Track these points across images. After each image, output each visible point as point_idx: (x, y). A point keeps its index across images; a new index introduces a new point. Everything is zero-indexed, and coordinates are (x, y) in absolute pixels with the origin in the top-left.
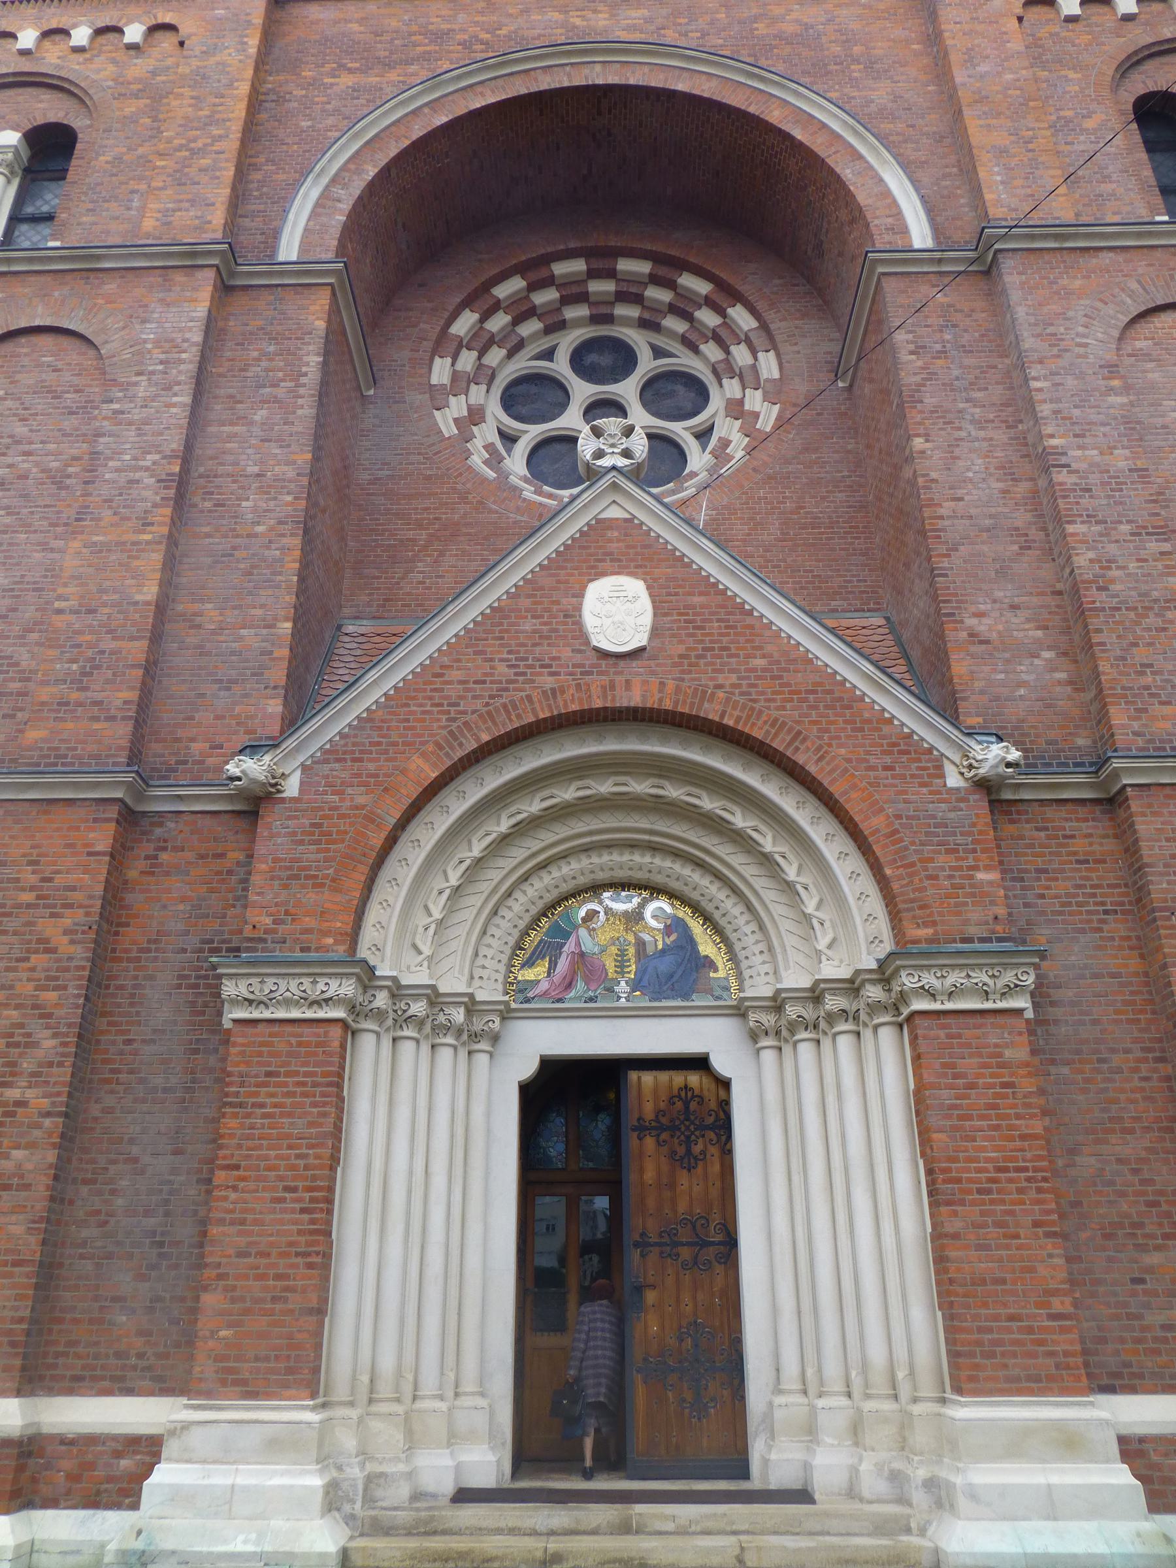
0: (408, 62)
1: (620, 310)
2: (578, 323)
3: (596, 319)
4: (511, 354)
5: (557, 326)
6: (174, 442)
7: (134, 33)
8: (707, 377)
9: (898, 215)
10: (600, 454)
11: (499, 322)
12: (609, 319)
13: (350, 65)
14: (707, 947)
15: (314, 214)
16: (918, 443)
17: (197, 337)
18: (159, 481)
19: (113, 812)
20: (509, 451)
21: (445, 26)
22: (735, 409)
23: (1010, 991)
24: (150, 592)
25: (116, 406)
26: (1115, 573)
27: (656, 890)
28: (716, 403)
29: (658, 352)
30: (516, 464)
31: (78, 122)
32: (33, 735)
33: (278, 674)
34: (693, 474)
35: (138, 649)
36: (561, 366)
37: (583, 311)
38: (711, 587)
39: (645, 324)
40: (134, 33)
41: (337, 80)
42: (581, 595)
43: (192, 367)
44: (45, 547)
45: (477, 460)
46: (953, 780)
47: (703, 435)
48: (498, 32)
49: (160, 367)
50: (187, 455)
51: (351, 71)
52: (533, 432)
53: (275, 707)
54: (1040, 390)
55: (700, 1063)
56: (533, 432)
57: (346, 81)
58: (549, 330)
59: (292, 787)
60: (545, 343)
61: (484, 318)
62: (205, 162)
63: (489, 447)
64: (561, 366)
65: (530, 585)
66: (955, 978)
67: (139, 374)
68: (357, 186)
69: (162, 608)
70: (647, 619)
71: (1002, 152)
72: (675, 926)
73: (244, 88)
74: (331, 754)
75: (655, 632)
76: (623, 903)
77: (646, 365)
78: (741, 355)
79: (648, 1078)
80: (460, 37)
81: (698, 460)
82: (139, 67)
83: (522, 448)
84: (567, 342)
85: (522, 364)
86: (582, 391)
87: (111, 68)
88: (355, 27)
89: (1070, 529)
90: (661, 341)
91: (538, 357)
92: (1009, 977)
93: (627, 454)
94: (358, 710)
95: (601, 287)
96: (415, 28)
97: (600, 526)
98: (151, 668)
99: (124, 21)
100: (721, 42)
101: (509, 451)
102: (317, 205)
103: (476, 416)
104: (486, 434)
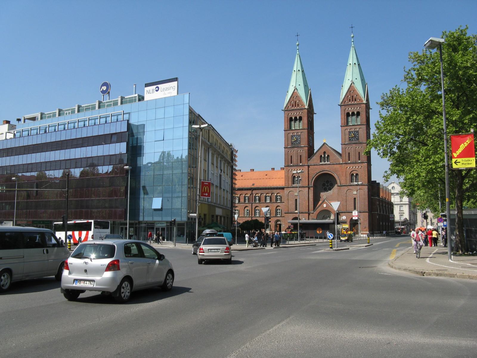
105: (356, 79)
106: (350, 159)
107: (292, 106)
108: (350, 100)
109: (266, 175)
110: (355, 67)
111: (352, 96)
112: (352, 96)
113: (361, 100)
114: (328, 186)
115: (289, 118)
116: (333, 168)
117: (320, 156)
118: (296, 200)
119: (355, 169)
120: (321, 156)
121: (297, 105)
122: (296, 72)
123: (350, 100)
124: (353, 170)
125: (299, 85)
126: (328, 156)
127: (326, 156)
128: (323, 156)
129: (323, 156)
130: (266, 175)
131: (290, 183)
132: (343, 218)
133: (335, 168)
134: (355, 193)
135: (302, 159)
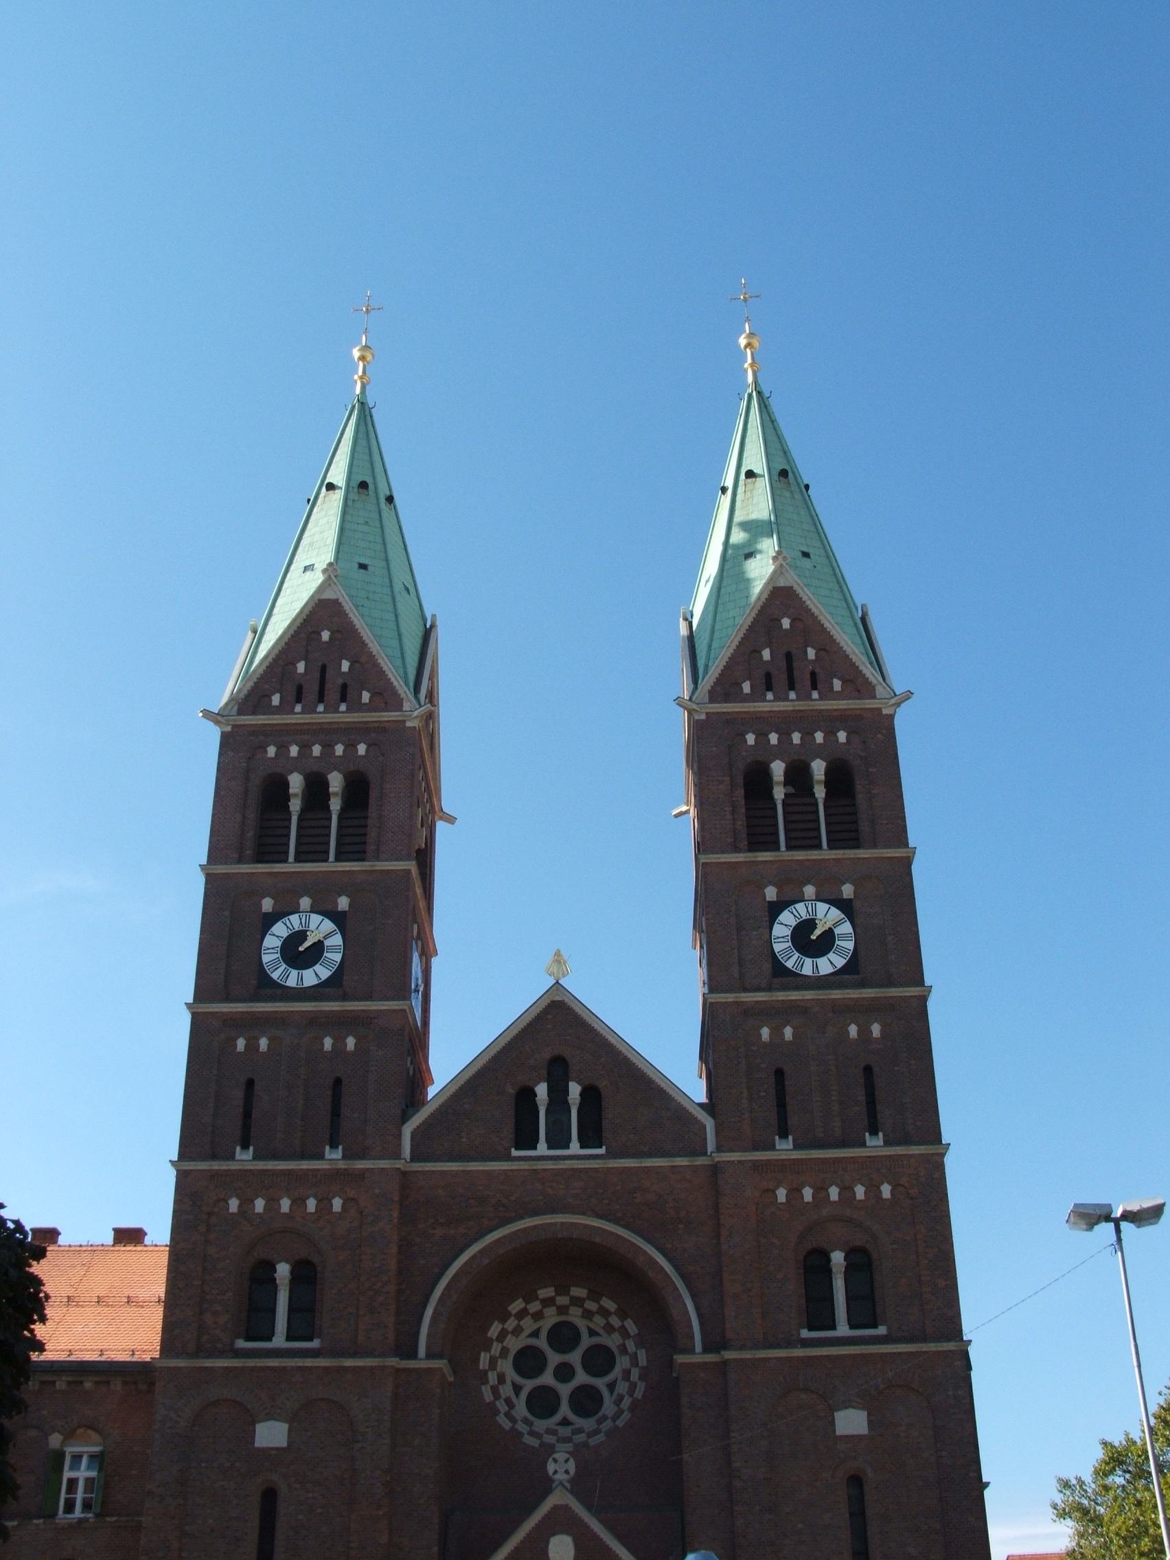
5: (538, 1316)
8: (616, 1351)
9: (690, 1326)
11: (511, 1324)
12: (567, 1313)
13: (440, 1221)
15: (430, 1326)
18: (383, 1485)
20: (517, 1395)
22: (626, 1374)
24: (384, 1539)
25: (360, 1445)
28: (617, 1372)
29: (592, 1333)
30: (521, 1409)
31: (316, 1259)
34: (605, 1418)
36: (542, 1343)
38: (596, 1537)
39: (583, 1317)
40: (337, 1204)
41: (435, 1231)
42: (548, 1542)
45: (502, 1420)
47: (611, 1386)
48: (511, 1198)
49: (376, 1424)
52: (529, 1385)
54: (734, 1437)
56: (529, 1385)
63: (508, 1402)
64: (542, 1343)
65: (529, 1537)
67: (368, 1427)
77: (586, 1341)
78: (631, 1346)
81: (608, 1407)
83: (524, 1395)
86: (554, 1359)
89: (736, 1508)
90: (592, 1326)
95: (562, 1300)
99: (331, 1195)
100: (618, 1207)
101: (517, 1395)
103: (501, 1379)
104: (507, 1390)
106: (793, 1120)
108: (768, 676)
110: (787, 494)
114: (565, 1372)
117: (511, 1091)
118: (270, 1496)
120: (527, 1095)
121: (332, 693)
122: (337, 497)
123: (768, 676)
124: (824, 1212)
125: (363, 567)
126: (591, 1095)
127: (575, 1090)
128: (542, 1090)
129: (542, 1090)
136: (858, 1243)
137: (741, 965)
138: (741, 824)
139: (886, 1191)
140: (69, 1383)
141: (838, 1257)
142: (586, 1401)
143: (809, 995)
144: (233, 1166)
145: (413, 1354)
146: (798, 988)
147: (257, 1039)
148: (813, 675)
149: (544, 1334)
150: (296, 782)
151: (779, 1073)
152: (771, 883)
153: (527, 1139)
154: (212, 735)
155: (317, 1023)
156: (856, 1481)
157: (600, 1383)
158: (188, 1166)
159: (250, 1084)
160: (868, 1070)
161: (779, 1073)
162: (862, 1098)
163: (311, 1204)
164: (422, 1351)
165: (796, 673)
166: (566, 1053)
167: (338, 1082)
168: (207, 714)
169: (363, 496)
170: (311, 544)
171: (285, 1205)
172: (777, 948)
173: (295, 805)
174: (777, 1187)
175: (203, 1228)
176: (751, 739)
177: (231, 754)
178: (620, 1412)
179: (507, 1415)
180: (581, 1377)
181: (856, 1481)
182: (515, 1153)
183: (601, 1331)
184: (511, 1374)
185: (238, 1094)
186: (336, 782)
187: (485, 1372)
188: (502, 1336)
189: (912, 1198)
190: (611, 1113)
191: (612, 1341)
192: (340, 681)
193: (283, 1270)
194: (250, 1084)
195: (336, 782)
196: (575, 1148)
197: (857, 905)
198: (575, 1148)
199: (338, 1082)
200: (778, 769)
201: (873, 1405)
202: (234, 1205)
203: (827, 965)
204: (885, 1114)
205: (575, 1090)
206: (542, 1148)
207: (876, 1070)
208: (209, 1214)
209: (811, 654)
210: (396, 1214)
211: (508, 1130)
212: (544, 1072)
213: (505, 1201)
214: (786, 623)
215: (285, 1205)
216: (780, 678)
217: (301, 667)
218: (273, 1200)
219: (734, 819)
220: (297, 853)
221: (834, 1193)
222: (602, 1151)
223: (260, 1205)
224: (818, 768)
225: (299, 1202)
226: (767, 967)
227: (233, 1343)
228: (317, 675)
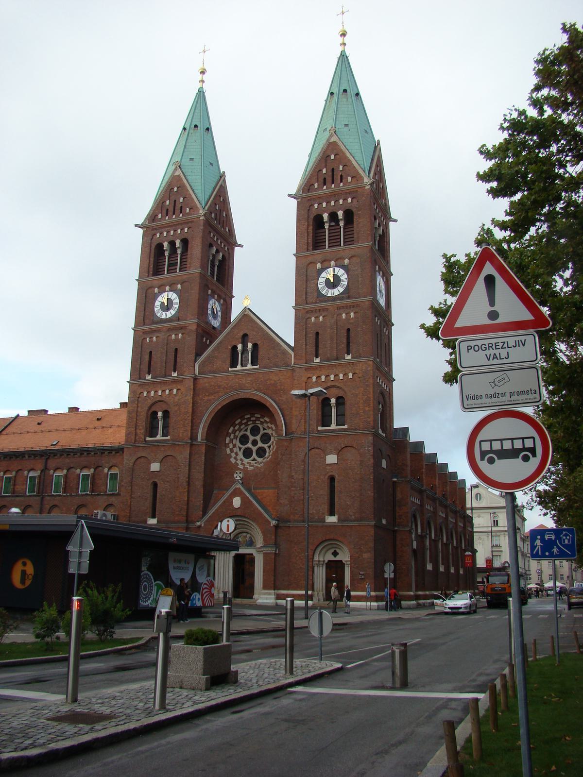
0: (215, 393)
1: (257, 422)
2: (251, 424)
3: (253, 423)
4: (240, 432)
6: (187, 476)
7: (175, 391)
10: (236, 477)
14: (253, 540)
15: (202, 430)
16: (279, 472)
17: (188, 457)
19: (185, 528)
21: (221, 384)
23: (273, 551)
24: (186, 499)
26: (296, 496)
27: (248, 533)
29: (264, 429)
31: (169, 410)
32: (176, 518)
33: (201, 509)
35: (185, 507)
37: (251, 422)
40: (175, 391)
43: (188, 462)
44: (174, 492)
46: (271, 525)
50: (189, 478)
51: (206, 396)
52: (244, 447)
53: (201, 513)
55: (252, 554)
56: (244, 447)
57: (206, 398)
58: (246, 426)
59: (203, 525)
60: (246, 428)
61: (234, 428)
62: (187, 422)
64: (248, 433)
65: (228, 498)
66: (267, 549)
68: (209, 422)
69: (188, 500)
70: (240, 504)
71: (297, 416)
72: (250, 538)
73: (191, 405)
74: (206, 521)
75: (241, 505)
76: (245, 534)
79: (248, 556)
80: (223, 386)
82: (177, 398)
83: (242, 450)
84: (250, 427)
85: (243, 433)
87: (173, 399)
88: (207, 385)
91: (245, 431)
92: (272, 549)
93: (240, 477)
94: (209, 515)
96: (216, 385)
97: (236, 488)
98: (188, 509)
102: (203, 427)
105: (346, 125)
106: (320, 352)
107: (165, 215)
108: (325, 179)
109: (98, 419)
110: (345, 100)
111: (333, 170)
112: (333, 170)
113: (356, 177)
114: (255, 443)
115: (153, 247)
116: (268, 382)
118: (155, 485)
119: (333, 384)
120: (235, 348)
123: (325, 179)
125: (191, 159)
126: (255, 346)
127: (250, 345)
128: (240, 347)
129: (240, 347)
130: (98, 419)
131: (141, 431)
132: (225, 530)
133: (272, 382)
134: (332, 459)
135: (178, 359)
136: (340, 395)
137: (306, 295)
138: (310, 240)
139: (350, 375)
140: (108, 453)
141: (333, 401)
142: (261, 453)
143: (329, 303)
144: (145, 381)
145: (196, 440)
146: (325, 301)
147: (152, 337)
148: (341, 176)
149: (249, 430)
150: (166, 245)
151: (317, 334)
152: (319, 262)
153: (234, 364)
154: (140, 231)
155: (170, 330)
156: (332, 479)
157: (265, 446)
158: (133, 382)
159: (151, 352)
160: (348, 330)
161: (317, 334)
162: (345, 341)
163: (167, 391)
164: (199, 439)
165: (335, 177)
166: (247, 332)
167: (176, 349)
168: (136, 226)
169: (196, 131)
170: (176, 154)
171: (160, 393)
172: (320, 287)
173: (167, 254)
174: (313, 376)
175: (136, 402)
176: (316, 206)
177: (146, 238)
178: (270, 456)
179: (235, 458)
180: (260, 444)
181: (332, 479)
182: (230, 369)
183: (267, 428)
184: (238, 444)
185: (147, 357)
186: (178, 243)
187: (229, 444)
188: (234, 432)
189: (359, 378)
190: (261, 352)
191: (269, 432)
192: (180, 206)
193: (160, 414)
194: (151, 352)
195: (178, 243)
196: (249, 366)
197: (350, 267)
198: (249, 366)
199: (176, 349)
200: (326, 216)
201: (339, 452)
202: (145, 394)
203: (337, 292)
204: (353, 346)
205: (250, 345)
206: (239, 367)
207: (351, 330)
208: (138, 398)
209: (341, 168)
210: (192, 393)
211: (228, 362)
212: (241, 340)
213: (226, 386)
214: (332, 157)
215: (160, 393)
216: (329, 179)
217: (168, 203)
218: (156, 391)
219: (308, 239)
220: (168, 270)
221: (332, 377)
222: (258, 367)
223: (152, 393)
224: (340, 214)
225: (163, 391)
226: (315, 294)
227: (145, 438)
228: (173, 205)
